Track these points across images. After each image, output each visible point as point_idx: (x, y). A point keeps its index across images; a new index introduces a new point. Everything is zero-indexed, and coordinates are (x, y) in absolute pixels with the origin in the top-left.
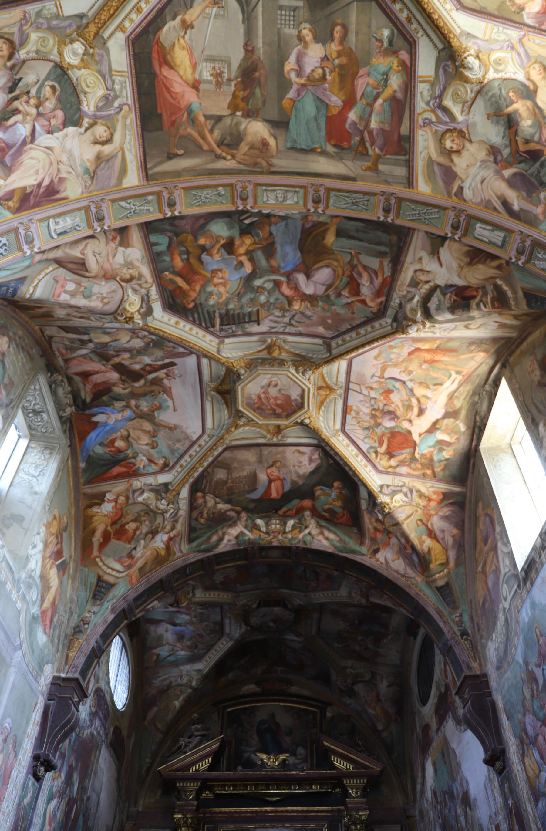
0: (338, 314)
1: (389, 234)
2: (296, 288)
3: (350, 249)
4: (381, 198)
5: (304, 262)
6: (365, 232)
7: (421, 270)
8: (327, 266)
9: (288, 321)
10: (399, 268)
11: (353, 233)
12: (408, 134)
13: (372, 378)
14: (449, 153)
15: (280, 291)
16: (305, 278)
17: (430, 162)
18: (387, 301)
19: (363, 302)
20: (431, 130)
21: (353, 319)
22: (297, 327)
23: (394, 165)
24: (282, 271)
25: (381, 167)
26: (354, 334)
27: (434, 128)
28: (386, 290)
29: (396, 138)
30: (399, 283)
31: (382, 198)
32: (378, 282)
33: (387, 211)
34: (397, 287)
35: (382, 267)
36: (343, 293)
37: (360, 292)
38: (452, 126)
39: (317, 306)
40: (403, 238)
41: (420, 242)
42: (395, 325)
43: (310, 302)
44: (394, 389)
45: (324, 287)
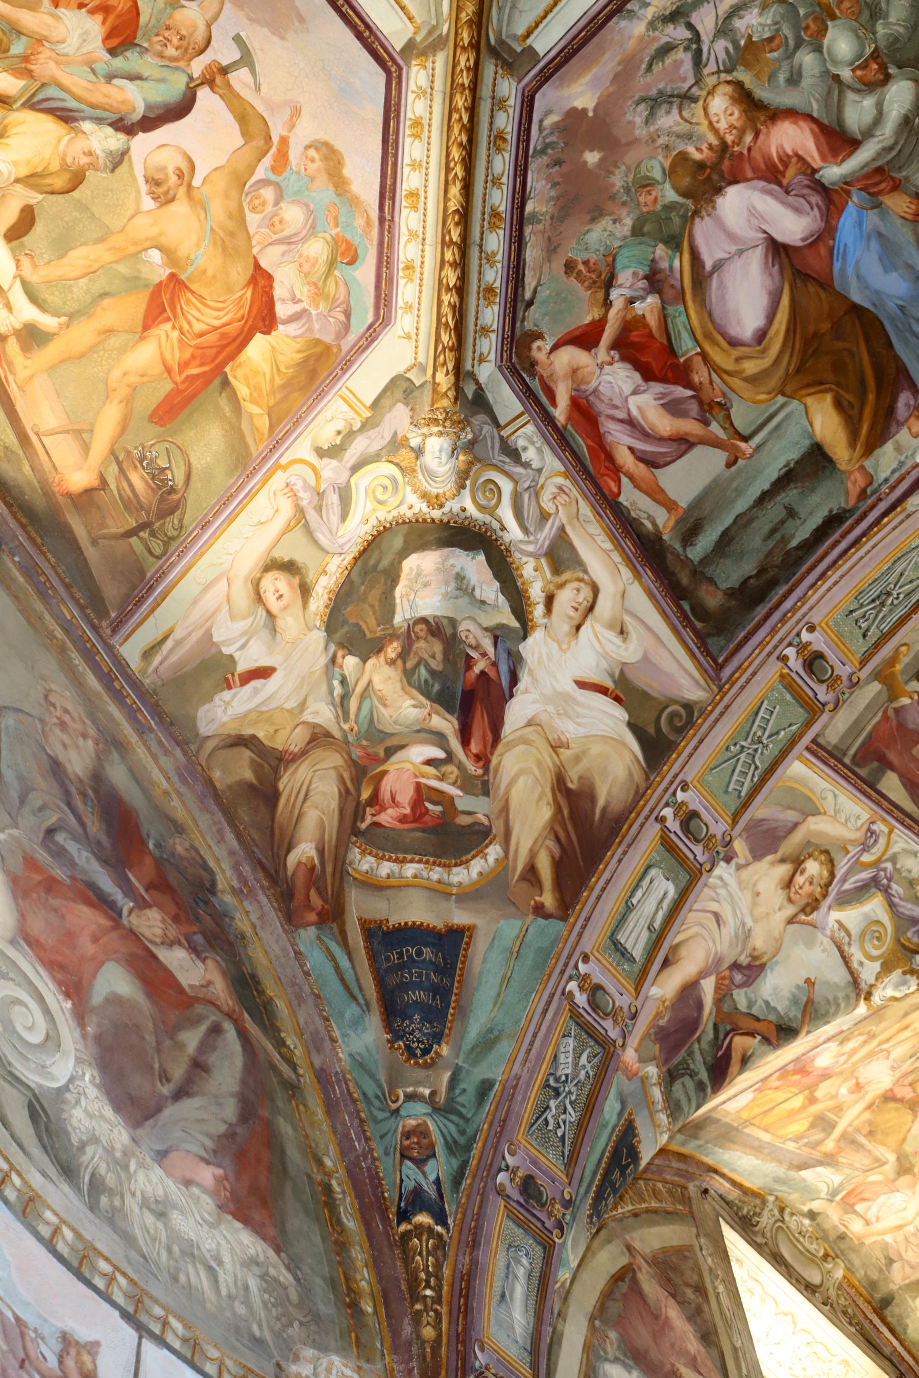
0: (597, 214)
1: (731, 593)
2: (772, 174)
3: (758, 448)
4: (848, 669)
5: (825, 283)
6: (773, 531)
7: (591, 609)
8: (761, 336)
9: (695, 18)
10: (628, 545)
11: (790, 495)
12: (881, 786)
13: (238, 39)
14: (797, 863)
15: (809, 117)
16: (779, 238)
17: (811, 809)
18: (548, 419)
19: (586, 339)
20: (852, 842)
21: (552, 249)
22: (652, 25)
23: (856, 722)
24: (856, 197)
25: (876, 687)
26: (500, 199)
27: (853, 851)
28: (582, 444)
29: (892, 756)
30: (585, 509)
31: (843, 671)
32: (621, 441)
33: (813, 662)
34: (575, 492)
35: (657, 494)
36: (652, 300)
37: (623, 358)
38: (833, 890)
39: (670, 173)
40: (699, 625)
41: (666, 664)
42: (469, 390)
43: (701, 166)
44: (118, 63)
45: (708, 266)
